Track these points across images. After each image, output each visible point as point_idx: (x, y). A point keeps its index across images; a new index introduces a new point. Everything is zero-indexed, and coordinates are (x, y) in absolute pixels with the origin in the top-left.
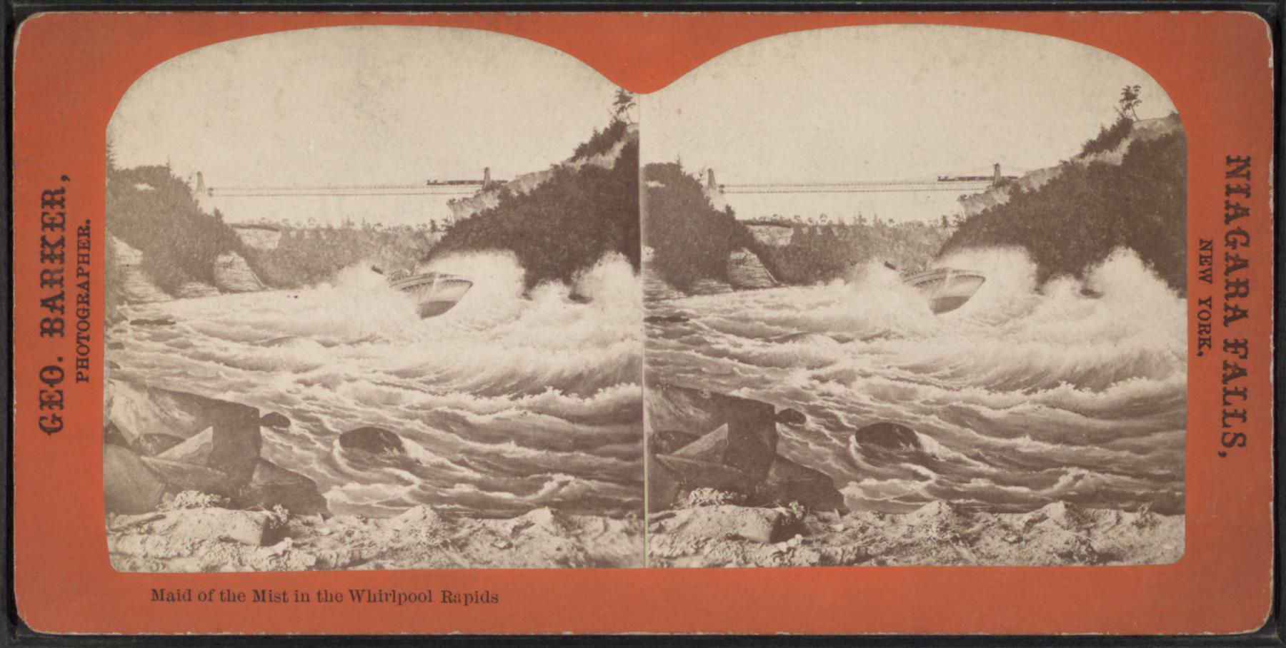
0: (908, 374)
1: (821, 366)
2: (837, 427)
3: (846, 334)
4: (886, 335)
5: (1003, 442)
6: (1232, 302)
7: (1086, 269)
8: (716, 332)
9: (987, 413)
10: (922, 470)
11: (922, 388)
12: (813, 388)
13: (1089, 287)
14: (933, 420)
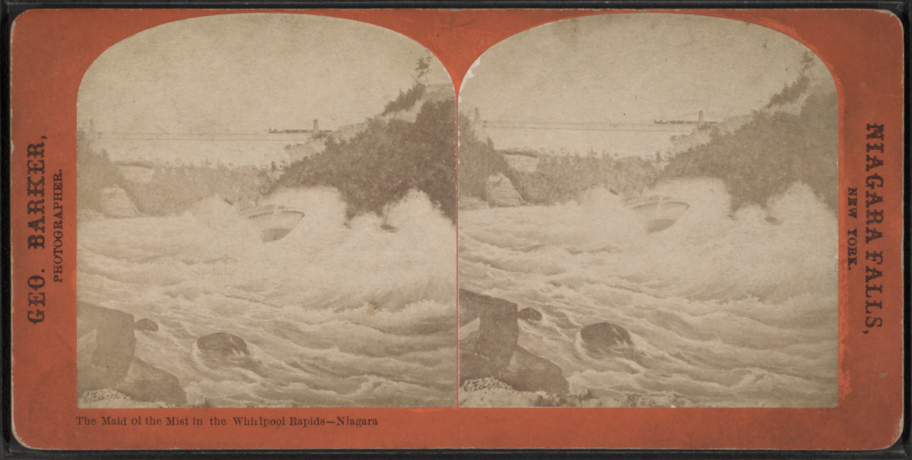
0: (625, 283)
1: (555, 273)
2: (566, 325)
3: (578, 248)
4: (607, 249)
5: (698, 343)
6: (871, 227)
7: (770, 200)
8: (474, 242)
9: (686, 318)
10: (634, 365)
11: (636, 295)
12: (550, 291)
13: (772, 215)
14: (643, 323)
